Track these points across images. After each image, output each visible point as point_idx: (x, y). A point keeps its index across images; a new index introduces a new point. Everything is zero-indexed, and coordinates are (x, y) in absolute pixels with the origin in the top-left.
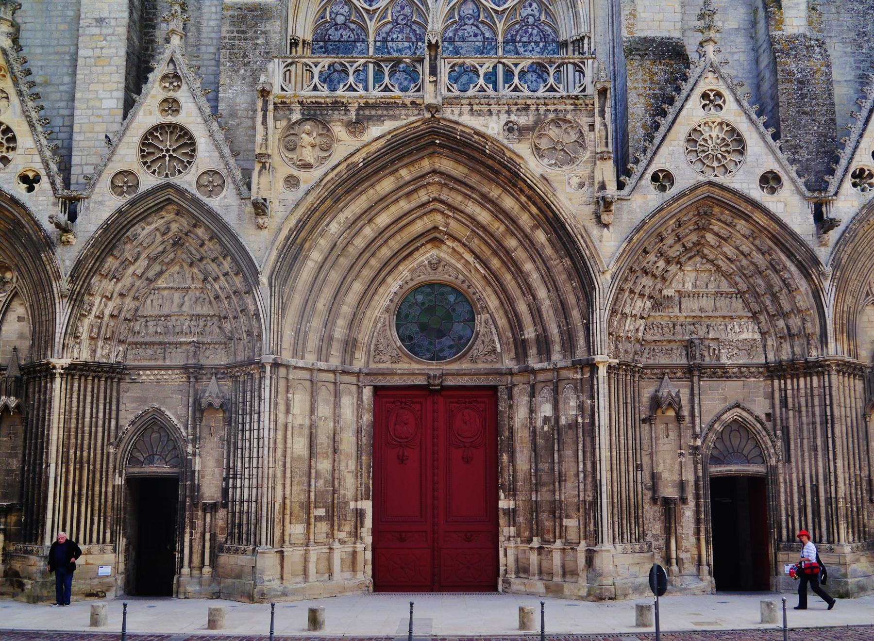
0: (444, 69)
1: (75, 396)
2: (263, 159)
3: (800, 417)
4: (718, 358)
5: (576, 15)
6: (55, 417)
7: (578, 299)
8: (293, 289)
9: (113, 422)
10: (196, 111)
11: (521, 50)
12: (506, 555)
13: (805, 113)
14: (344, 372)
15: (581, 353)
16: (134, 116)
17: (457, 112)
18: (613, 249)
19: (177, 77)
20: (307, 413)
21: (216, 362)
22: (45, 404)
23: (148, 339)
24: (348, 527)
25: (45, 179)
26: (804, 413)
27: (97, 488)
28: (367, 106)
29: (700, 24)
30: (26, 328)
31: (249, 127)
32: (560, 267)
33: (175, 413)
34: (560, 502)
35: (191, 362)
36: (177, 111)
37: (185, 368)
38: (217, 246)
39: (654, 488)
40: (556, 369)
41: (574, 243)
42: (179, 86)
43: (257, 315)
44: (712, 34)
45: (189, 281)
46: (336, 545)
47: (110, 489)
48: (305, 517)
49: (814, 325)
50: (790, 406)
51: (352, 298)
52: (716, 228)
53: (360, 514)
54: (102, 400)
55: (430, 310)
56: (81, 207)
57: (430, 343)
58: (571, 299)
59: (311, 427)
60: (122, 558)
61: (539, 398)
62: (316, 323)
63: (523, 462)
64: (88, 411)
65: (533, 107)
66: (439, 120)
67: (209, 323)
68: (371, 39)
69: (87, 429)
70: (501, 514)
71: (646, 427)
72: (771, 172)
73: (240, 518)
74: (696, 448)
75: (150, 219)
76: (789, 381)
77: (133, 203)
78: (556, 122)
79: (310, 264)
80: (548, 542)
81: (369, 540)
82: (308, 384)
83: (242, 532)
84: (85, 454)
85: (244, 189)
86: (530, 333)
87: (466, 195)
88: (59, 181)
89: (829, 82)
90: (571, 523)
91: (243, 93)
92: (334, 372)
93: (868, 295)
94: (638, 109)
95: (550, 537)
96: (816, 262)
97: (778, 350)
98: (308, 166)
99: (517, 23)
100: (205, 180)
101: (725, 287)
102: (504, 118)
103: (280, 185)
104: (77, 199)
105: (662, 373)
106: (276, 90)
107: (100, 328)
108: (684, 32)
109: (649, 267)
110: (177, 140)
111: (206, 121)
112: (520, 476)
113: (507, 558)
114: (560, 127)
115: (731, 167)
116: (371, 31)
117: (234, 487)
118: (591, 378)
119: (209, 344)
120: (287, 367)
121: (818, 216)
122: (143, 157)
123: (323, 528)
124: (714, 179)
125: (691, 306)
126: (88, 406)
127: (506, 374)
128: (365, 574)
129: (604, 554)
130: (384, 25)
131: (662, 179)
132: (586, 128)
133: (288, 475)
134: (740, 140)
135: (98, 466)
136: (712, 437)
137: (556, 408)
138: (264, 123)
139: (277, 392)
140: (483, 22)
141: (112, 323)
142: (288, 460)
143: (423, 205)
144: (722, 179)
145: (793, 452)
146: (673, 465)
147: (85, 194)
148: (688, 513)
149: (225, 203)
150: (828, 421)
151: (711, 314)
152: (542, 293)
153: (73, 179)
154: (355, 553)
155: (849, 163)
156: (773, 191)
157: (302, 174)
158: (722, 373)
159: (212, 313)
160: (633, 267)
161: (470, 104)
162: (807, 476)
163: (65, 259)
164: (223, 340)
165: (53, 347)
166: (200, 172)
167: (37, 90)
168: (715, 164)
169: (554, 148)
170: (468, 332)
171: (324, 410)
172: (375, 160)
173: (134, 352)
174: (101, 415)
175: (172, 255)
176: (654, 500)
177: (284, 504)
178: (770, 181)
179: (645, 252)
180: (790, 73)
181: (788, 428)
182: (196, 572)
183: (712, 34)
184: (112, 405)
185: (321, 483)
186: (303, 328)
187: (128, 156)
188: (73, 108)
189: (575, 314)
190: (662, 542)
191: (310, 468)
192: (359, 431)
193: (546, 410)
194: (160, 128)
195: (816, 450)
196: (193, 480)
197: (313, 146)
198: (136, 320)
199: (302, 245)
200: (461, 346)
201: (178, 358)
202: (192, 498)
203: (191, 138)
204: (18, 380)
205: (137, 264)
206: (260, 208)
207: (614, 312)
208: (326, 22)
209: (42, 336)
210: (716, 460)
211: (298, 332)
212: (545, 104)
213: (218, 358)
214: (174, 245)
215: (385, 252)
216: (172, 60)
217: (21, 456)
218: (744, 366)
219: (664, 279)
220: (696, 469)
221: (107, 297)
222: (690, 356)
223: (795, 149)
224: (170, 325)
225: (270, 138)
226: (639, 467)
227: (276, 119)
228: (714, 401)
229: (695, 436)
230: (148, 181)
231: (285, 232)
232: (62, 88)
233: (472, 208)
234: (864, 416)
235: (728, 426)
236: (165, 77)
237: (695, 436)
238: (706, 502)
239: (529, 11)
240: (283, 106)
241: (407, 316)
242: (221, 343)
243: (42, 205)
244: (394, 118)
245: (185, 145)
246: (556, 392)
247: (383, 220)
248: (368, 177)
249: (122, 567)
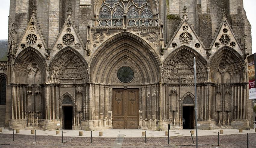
0: (127, 21)
1: (51, 90)
2: (89, 41)
3: (202, 94)
4: (185, 82)
5: (156, 9)
6: (47, 94)
7: (156, 70)
8: (95, 68)
9: (59, 95)
10: (74, 31)
11: (144, 17)
12: (140, 122)
13: (206, 31)
14: (106, 85)
15: (156, 82)
16: (61, 32)
17: (130, 31)
18: (163, 60)
19: (70, 24)
20: (99, 93)
21: (80, 83)
22: (45, 92)
23: (65, 79)
24: (108, 116)
25: (43, 46)
26: (203, 94)
27: (56, 108)
28: (111, 29)
29: (183, 11)
30: (40, 76)
31: (85, 34)
32: (152, 63)
33: (71, 94)
34: (151, 111)
35: (74, 83)
36: (70, 31)
37: (73, 84)
38: (80, 60)
39: (171, 109)
40: (152, 85)
41: (155, 58)
42: (70, 26)
43: (88, 74)
44: (186, 14)
45: (74, 67)
46: (105, 120)
47: (59, 109)
48: (98, 114)
49: (205, 76)
50: (200, 92)
51: (108, 70)
52: (186, 55)
53: (110, 114)
54: (56, 91)
55: (125, 72)
57: (125, 79)
58: (154, 70)
59: (99, 96)
60: (62, 122)
61: (147, 91)
62: (100, 75)
63: (144, 104)
64: (54, 93)
65: (147, 30)
66: (126, 32)
68: (112, 14)
69: (54, 97)
70: (139, 114)
71: (170, 96)
72: (198, 43)
73: (85, 115)
74: (180, 101)
75: (65, 54)
76: (200, 87)
77: (61, 51)
78: (151, 33)
79: (99, 63)
80: (149, 120)
81: (112, 119)
82: (99, 88)
83: (86, 117)
84: (53, 102)
85: (85, 48)
86: (145, 77)
87: (132, 48)
88: (46, 46)
89: (211, 24)
90: (153, 116)
91: (84, 27)
92: (104, 85)
93: (217, 69)
94: (169, 30)
95: (149, 119)
96: (206, 63)
97: (197, 80)
98: (98, 42)
99: (143, 11)
101: (187, 67)
102: (140, 32)
103: (92, 46)
104: (50, 50)
105: (172, 85)
106: (91, 26)
107: (55, 76)
108: (180, 13)
109: (171, 63)
110: (70, 37)
111: (76, 33)
112: (143, 106)
113: (140, 123)
114: (152, 34)
115: (189, 42)
116: (112, 13)
117: (84, 108)
118: (158, 86)
120: (94, 84)
121: (207, 53)
122: (63, 41)
123: (102, 117)
124: (185, 45)
125: (180, 72)
126: (54, 92)
127: (140, 86)
128: (111, 126)
129: (160, 122)
130: (115, 11)
131: (174, 45)
132: (158, 34)
133: (95, 106)
134: (191, 37)
135: (56, 104)
136: (183, 98)
137: (151, 93)
138: (89, 33)
139: (92, 89)
140: (136, 11)
141: (58, 75)
142: (95, 103)
143: (123, 50)
144: (187, 45)
145: (200, 102)
146: (175, 104)
147: (51, 49)
148: (178, 114)
149: (80, 51)
150: (208, 95)
151: (184, 73)
152: (148, 69)
153: (49, 46)
154: (109, 121)
156: (198, 47)
157: (97, 44)
158: (186, 85)
160: (167, 63)
161: (133, 29)
162: (203, 106)
163: (48, 63)
164: (81, 79)
165: (46, 80)
166: (75, 44)
167: (41, 27)
168: (186, 42)
169: (151, 38)
170: (133, 77)
171: (102, 93)
172: (113, 41)
174: (56, 94)
175: (70, 61)
176: (171, 111)
177: (94, 112)
178: (197, 45)
179: (170, 60)
181: (199, 97)
182: (77, 125)
183: (186, 14)
184: (59, 93)
185: (102, 107)
186: (97, 76)
187: (60, 41)
188: (48, 31)
189: (155, 73)
190: (172, 119)
191: (99, 105)
192: (109, 97)
193: (149, 93)
195: (205, 101)
196: (75, 107)
199: (97, 59)
200: (131, 80)
201: (72, 83)
202: (75, 111)
203: (73, 37)
204: (39, 87)
206: (88, 52)
207: (163, 73)
208: (102, 11)
209: (44, 78)
210: (184, 103)
211: (96, 77)
212: (149, 29)
213: (80, 82)
214: (70, 59)
215: (115, 60)
216: (69, 20)
217: (40, 102)
218: (190, 84)
219: (174, 66)
220: (180, 105)
221: (56, 70)
222: (179, 82)
223: (203, 38)
224: (70, 76)
225: (90, 37)
226: (168, 105)
227: (91, 33)
228: (184, 91)
229: (180, 98)
230: (64, 46)
231: (93, 57)
232: (46, 26)
233: (133, 51)
234: (215, 94)
235: (187, 96)
236: (68, 24)
237: (180, 98)
238: (182, 111)
239: (146, 8)
240: (92, 29)
241: (120, 74)
243: (42, 51)
244: (117, 32)
245: (72, 38)
246: (151, 89)
247: (114, 54)
248: (111, 45)
249: (62, 124)
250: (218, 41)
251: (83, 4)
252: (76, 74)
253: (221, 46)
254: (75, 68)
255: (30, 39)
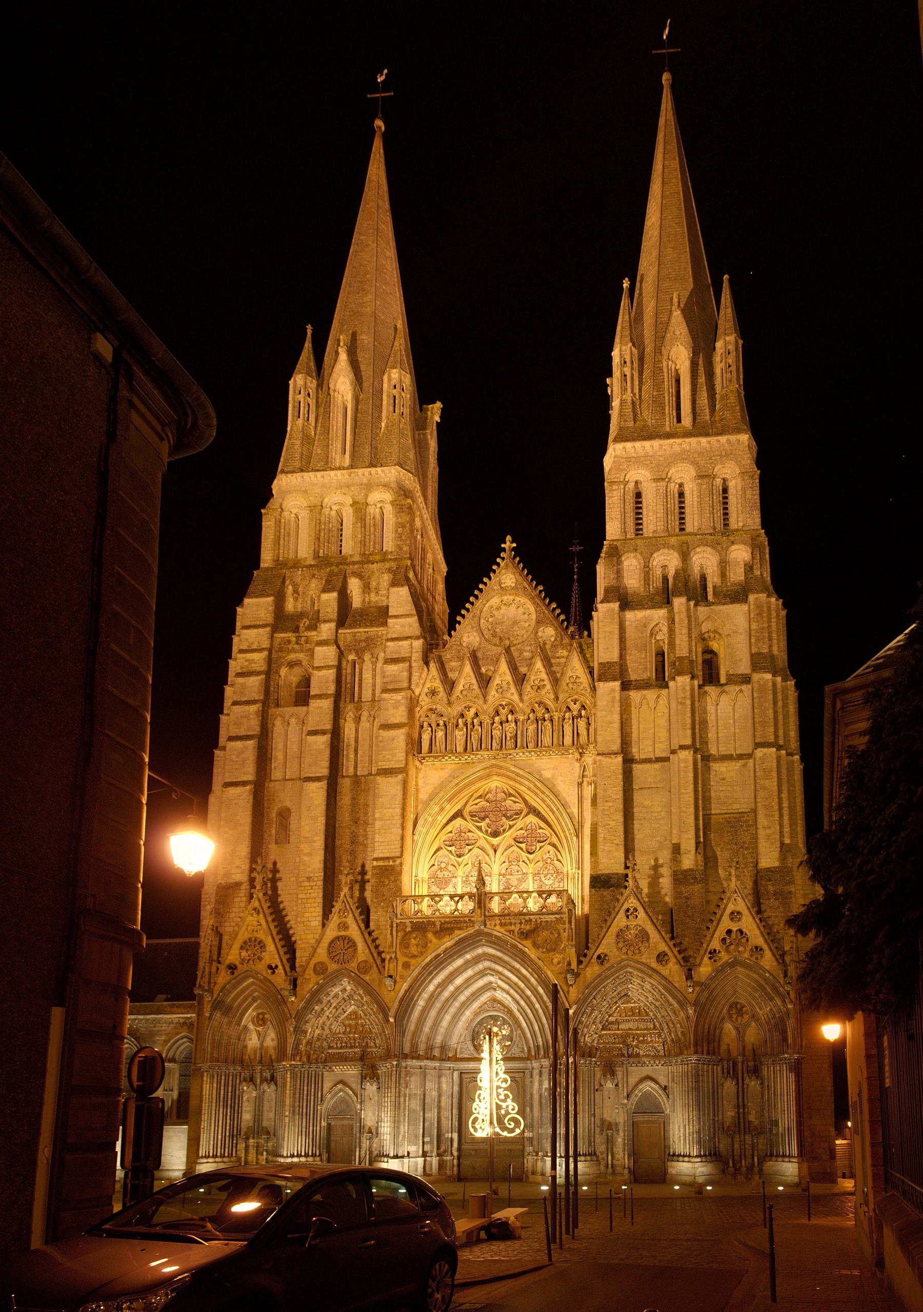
11: (543, 879)
56: (298, 982)
98: (414, 956)
100: (362, 965)
102: (518, 926)
103: (400, 967)
155: (708, 946)
157: (413, 961)
180: (681, 893)
187: (322, 954)
194: (338, 938)
197: (417, 945)
250: (716, 944)
251: (381, 855)
253: (724, 957)
255: (247, 950)
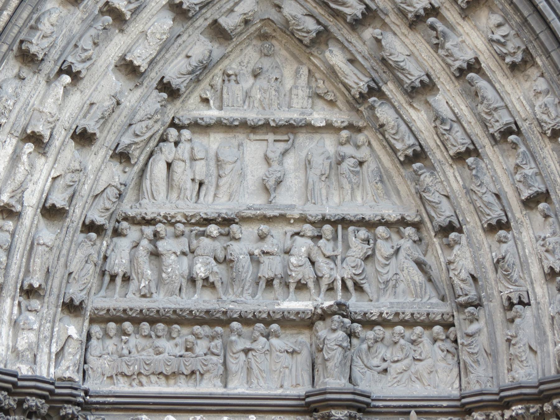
23: (162, 301)
67: (384, 248)
119: (385, 323)
141: (47, 234)
159: (393, 215)
164: (440, 309)
173: (111, 345)
198: (117, 233)
205: (134, 29)
224: (239, 250)
242: (428, 325)
252: (345, 222)
254: (329, 127)
